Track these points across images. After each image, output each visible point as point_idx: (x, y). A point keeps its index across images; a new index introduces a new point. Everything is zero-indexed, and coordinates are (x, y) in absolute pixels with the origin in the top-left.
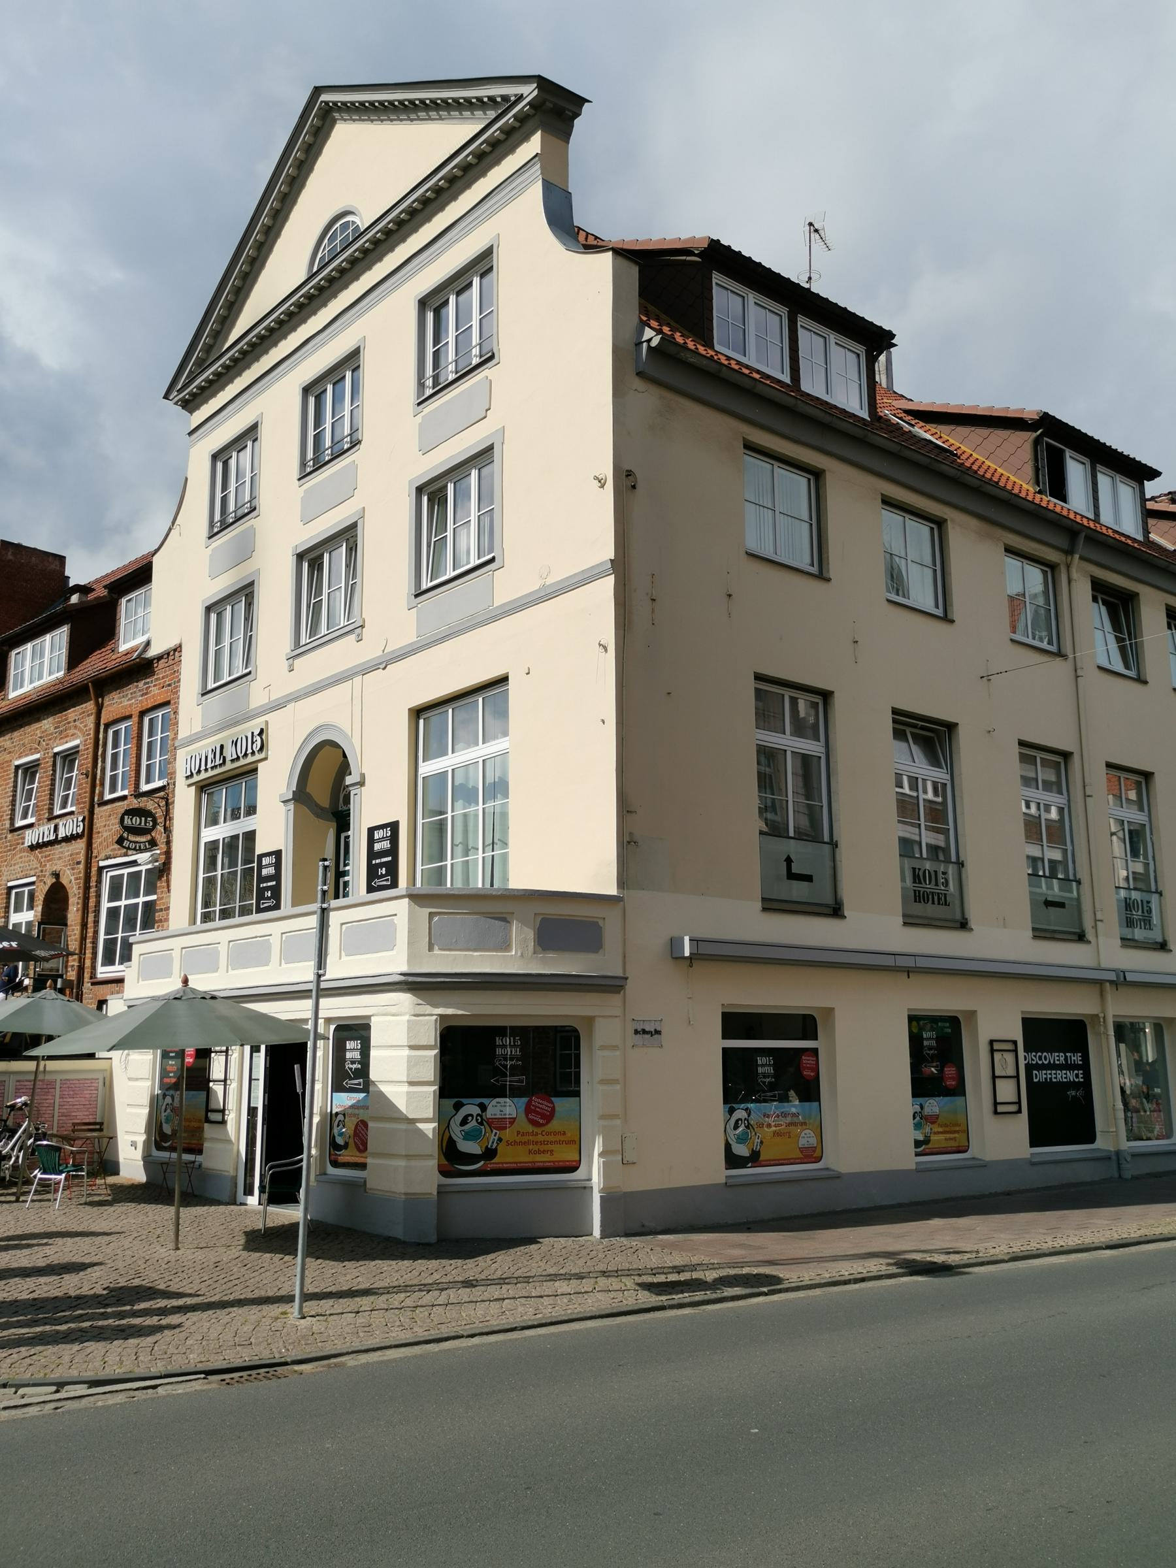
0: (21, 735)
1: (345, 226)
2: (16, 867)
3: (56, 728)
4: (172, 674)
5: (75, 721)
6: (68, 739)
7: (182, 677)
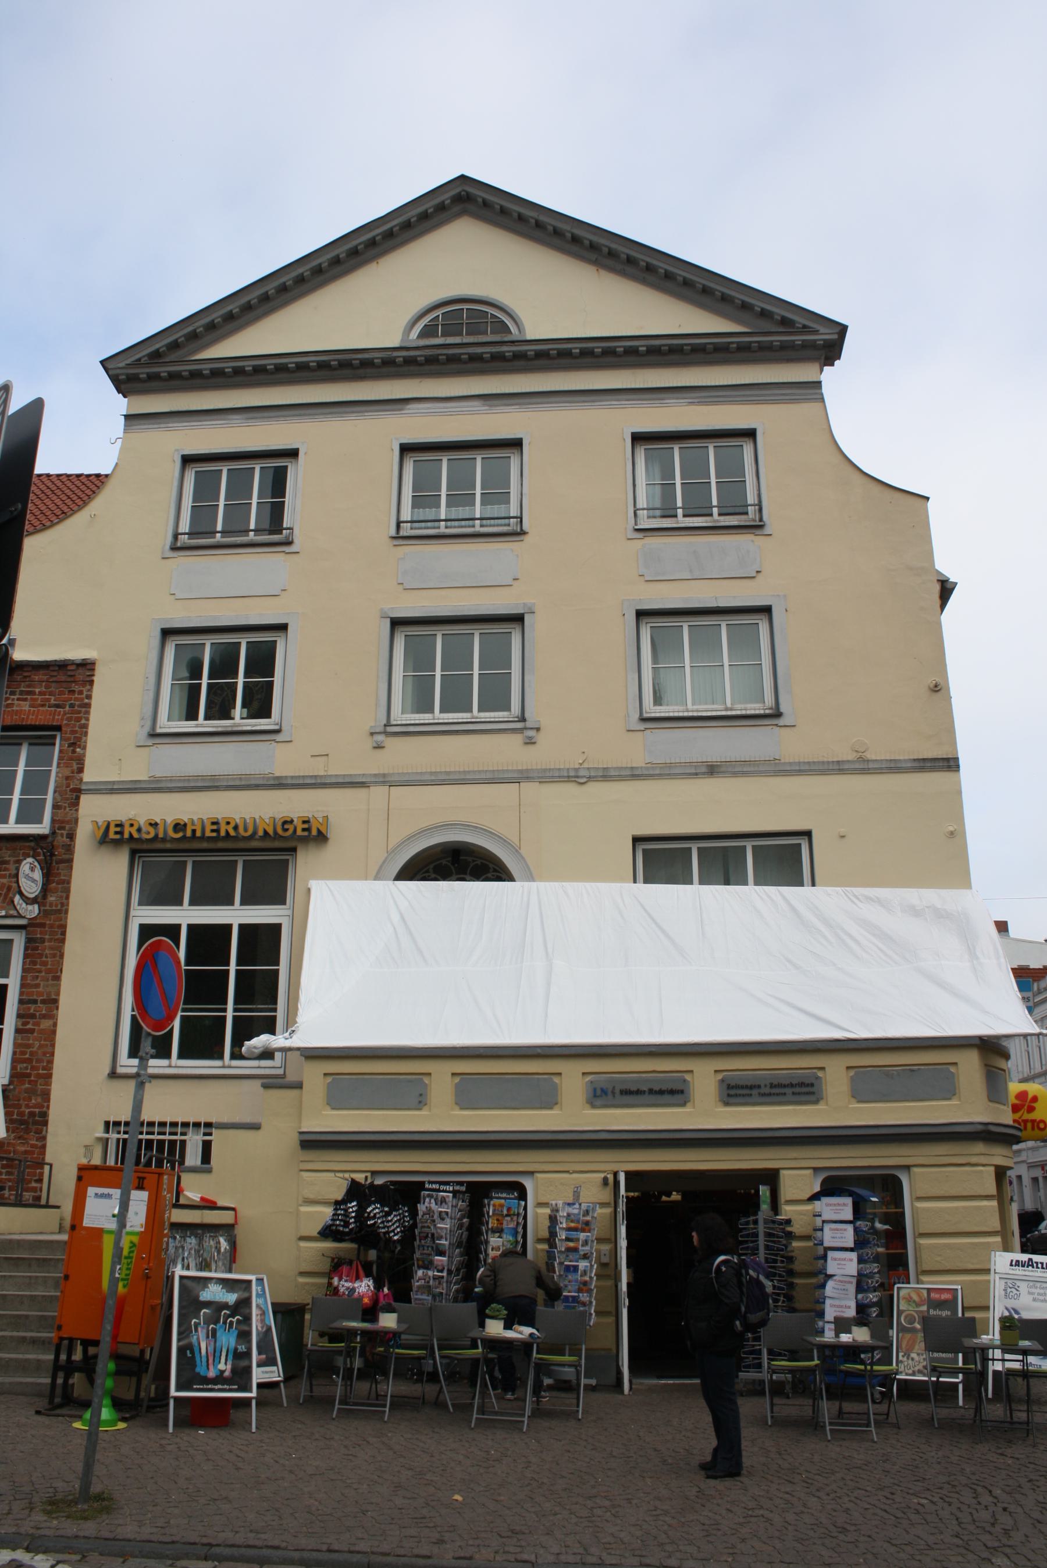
7: (95, 702)
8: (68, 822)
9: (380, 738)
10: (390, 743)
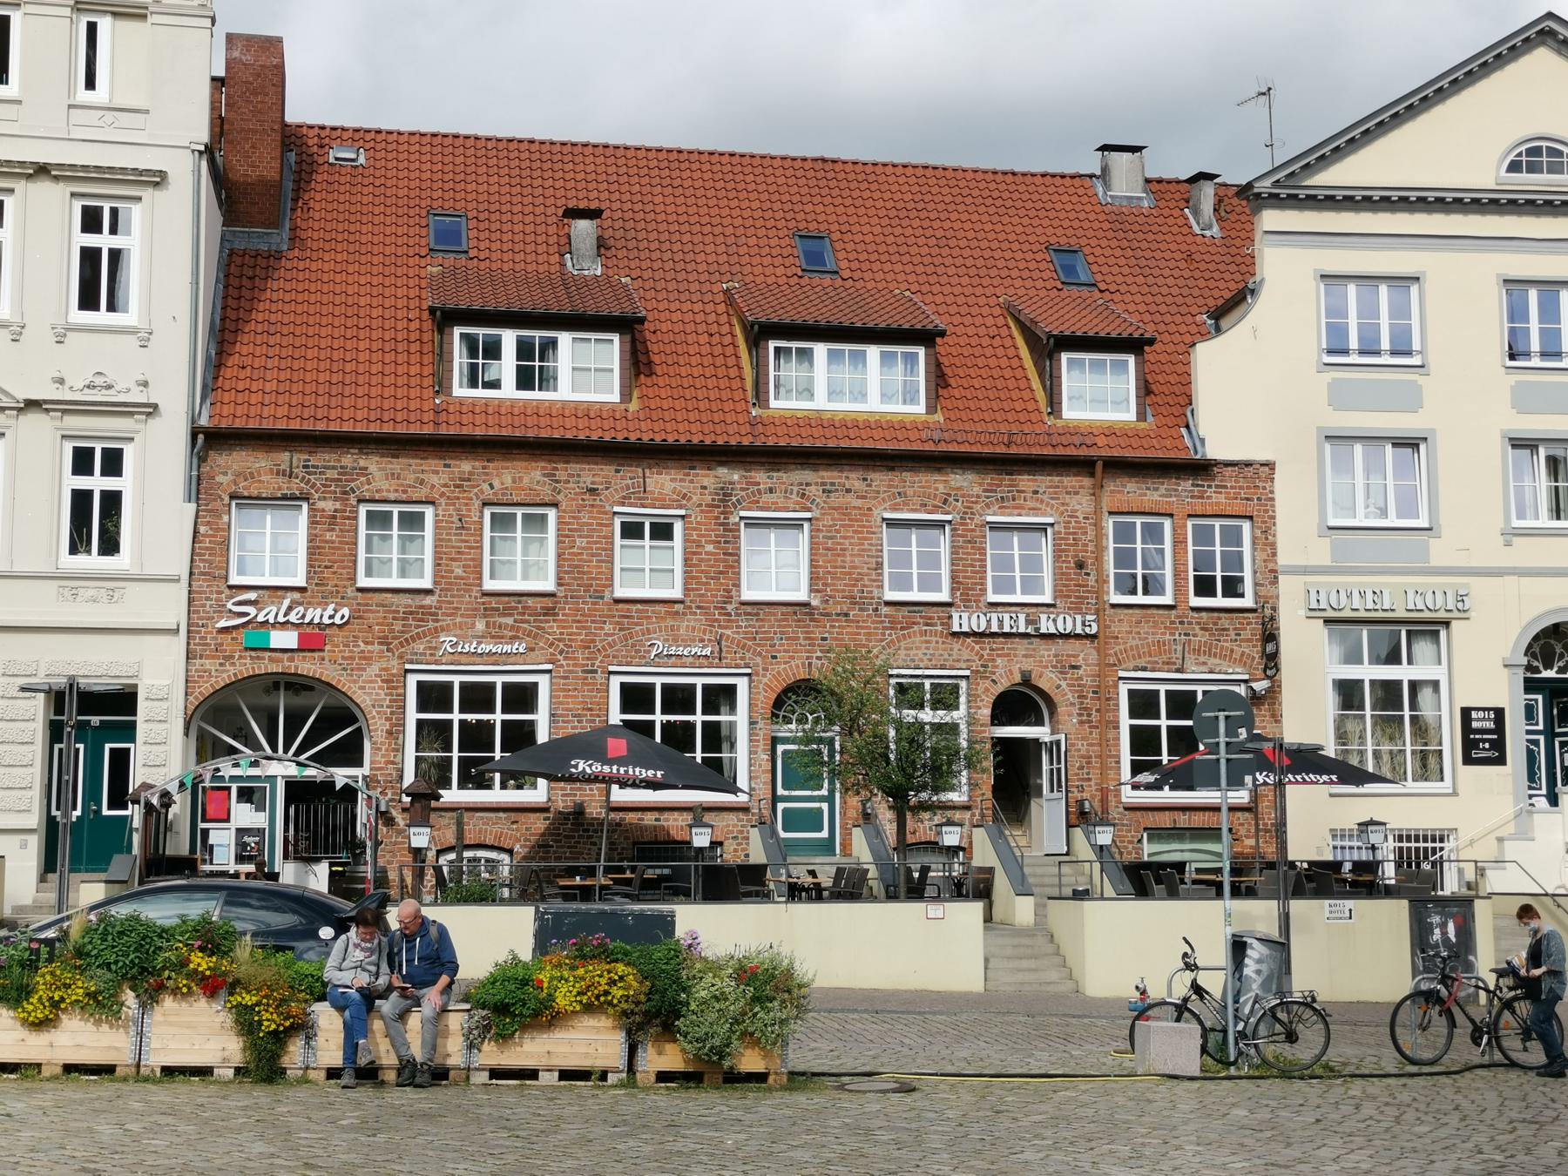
0: (890, 480)
2: (912, 653)
4: (1248, 488)
5: (1036, 492)
6: (1023, 512)
7: (1278, 495)
8: (1271, 597)
9: (1508, 537)
10: (1516, 540)
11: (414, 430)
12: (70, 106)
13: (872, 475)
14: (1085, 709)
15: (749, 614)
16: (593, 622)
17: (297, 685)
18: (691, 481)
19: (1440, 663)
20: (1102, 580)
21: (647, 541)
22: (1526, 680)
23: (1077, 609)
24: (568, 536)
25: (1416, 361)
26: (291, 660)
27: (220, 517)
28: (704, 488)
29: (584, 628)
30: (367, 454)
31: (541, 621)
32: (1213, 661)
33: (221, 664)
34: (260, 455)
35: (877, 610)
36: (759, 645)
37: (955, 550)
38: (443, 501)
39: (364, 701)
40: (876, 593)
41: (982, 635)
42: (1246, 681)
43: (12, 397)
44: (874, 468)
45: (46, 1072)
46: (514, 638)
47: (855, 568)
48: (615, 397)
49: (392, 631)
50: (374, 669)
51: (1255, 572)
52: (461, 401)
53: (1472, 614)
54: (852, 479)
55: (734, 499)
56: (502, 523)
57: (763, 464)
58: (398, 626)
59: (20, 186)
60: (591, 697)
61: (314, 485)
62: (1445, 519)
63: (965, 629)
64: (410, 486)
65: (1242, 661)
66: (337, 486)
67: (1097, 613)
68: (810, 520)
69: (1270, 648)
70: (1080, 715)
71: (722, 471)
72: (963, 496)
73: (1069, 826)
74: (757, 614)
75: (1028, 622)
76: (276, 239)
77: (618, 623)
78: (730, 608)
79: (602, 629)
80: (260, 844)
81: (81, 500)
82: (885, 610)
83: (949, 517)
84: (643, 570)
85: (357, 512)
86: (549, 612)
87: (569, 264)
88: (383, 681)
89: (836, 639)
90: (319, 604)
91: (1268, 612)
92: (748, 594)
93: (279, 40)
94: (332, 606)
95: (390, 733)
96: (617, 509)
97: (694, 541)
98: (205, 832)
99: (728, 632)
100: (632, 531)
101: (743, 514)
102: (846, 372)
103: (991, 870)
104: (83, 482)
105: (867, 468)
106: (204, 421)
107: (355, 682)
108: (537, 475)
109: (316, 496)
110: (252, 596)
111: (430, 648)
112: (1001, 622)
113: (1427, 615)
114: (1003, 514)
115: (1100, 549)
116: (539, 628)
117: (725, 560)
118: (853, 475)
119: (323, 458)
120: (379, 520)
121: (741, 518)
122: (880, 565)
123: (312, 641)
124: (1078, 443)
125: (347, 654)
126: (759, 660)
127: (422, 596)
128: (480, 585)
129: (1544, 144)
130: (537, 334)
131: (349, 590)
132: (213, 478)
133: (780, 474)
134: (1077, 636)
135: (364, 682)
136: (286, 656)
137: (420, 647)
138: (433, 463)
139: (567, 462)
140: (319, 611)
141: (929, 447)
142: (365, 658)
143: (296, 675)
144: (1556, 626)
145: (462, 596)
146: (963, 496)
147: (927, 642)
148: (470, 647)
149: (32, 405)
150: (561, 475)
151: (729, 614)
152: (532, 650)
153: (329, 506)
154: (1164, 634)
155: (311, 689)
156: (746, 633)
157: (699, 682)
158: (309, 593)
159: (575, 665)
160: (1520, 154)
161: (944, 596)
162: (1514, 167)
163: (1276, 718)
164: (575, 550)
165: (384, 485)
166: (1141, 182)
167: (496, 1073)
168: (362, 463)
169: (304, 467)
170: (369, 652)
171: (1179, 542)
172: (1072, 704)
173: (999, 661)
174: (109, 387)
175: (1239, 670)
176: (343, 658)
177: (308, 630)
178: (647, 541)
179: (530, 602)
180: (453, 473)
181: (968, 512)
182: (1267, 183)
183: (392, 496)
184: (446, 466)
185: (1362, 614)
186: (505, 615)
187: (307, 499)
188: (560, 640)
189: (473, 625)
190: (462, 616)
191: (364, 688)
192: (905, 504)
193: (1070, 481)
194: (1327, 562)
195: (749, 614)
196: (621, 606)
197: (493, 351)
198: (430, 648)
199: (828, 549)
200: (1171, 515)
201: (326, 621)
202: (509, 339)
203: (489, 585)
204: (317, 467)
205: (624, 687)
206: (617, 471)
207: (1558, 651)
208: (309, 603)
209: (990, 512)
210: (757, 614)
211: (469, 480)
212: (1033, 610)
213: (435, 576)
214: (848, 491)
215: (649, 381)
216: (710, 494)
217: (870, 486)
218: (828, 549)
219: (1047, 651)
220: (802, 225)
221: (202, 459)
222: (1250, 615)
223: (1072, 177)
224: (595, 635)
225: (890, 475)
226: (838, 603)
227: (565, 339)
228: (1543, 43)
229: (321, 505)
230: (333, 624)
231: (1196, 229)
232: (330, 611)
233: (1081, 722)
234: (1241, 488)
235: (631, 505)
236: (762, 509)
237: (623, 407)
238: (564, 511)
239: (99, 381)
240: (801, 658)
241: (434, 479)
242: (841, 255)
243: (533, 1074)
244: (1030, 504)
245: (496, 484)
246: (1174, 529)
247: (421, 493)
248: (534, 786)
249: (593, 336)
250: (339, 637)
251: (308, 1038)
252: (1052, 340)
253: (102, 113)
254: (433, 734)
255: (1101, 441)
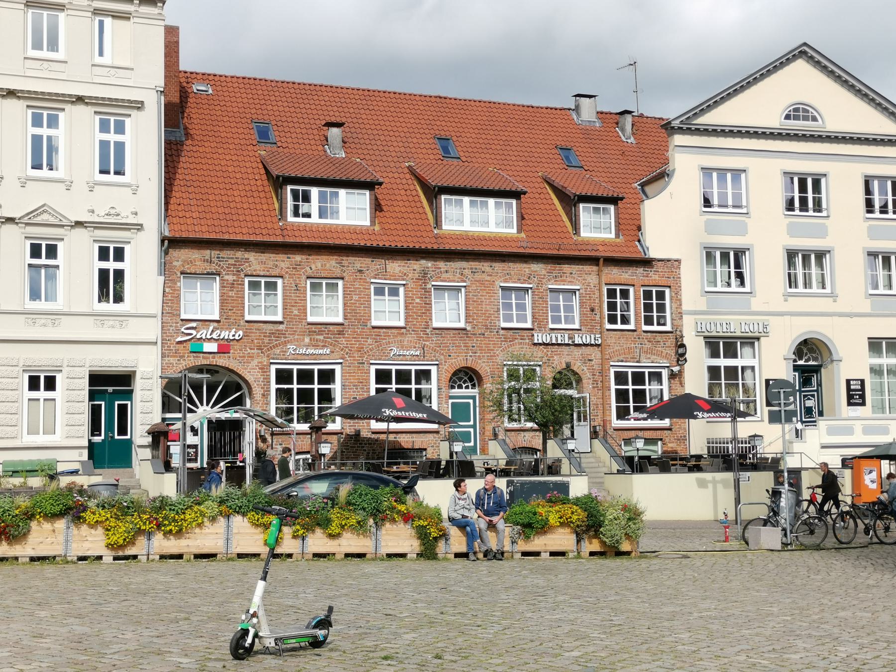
1: (808, 111)
3: (548, 272)
5: (571, 273)
7: (682, 276)
10: (790, 298)
11: (272, 239)
12: (93, 65)
13: (494, 264)
14: (595, 381)
15: (436, 334)
16: (362, 338)
17: (211, 370)
18: (408, 267)
19: (754, 357)
20: (602, 317)
21: (387, 297)
22: (794, 366)
23: (591, 331)
24: (349, 294)
25: (744, 211)
26: (214, 358)
27: (176, 284)
28: (415, 270)
29: (358, 341)
30: (248, 251)
31: (337, 338)
32: (653, 357)
33: (178, 360)
34: (196, 251)
35: (497, 332)
36: (442, 350)
37: (534, 302)
38: (287, 276)
39: (250, 379)
40: (497, 324)
41: (547, 344)
42: (668, 367)
43: (68, 219)
44: (496, 261)
45: (338, 557)
46: (324, 346)
47: (487, 311)
48: (368, 223)
49: (263, 343)
50: (255, 362)
51: (672, 314)
52: (293, 224)
53: (770, 334)
54: (485, 266)
55: (429, 276)
56: (315, 287)
57: (442, 258)
58: (266, 340)
59: (68, 107)
60: (362, 376)
61: (223, 267)
62: (758, 289)
63: (540, 341)
64: (270, 268)
65: (666, 357)
66: (234, 268)
67: (601, 333)
68: (465, 287)
69: (681, 351)
70: (593, 384)
71: (423, 262)
72: (537, 275)
73: (591, 438)
74: (441, 334)
75: (569, 338)
76: (178, 134)
77: (374, 339)
78: (428, 331)
79: (367, 341)
80: (196, 453)
81: (103, 275)
82: (502, 332)
83: (531, 286)
84: (385, 312)
85: (244, 281)
86: (341, 333)
87: (328, 151)
88: (259, 368)
89: (479, 347)
90: (227, 329)
91: (678, 333)
92: (436, 324)
93: (178, 28)
94: (234, 330)
95: (263, 395)
96: (373, 280)
97: (410, 297)
98: (168, 447)
99: (427, 343)
100: (379, 292)
101: (433, 283)
102: (479, 212)
103: (559, 460)
104: (104, 265)
105: (492, 261)
106: (167, 234)
107: (246, 369)
108: (333, 263)
109: (224, 273)
110: (194, 325)
111: (283, 351)
112: (557, 338)
113: (750, 334)
114: (556, 284)
115: (601, 301)
116: (336, 341)
117: (425, 307)
118: (486, 264)
119: (226, 253)
120: (254, 286)
121: (433, 285)
122: (499, 309)
123: (224, 349)
124: (590, 249)
125: (241, 355)
126: (442, 357)
127: (278, 325)
128: (306, 319)
129: (801, 106)
130: (329, 190)
131: (242, 322)
132: (172, 263)
133: (451, 263)
134: (592, 345)
135: (250, 369)
136: (211, 356)
137: (277, 351)
138: (281, 257)
139: (348, 256)
140: (227, 333)
141: (521, 251)
142: (250, 357)
143: (216, 365)
144: (805, 341)
145: (298, 325)
146: (537, 275)
147: (522, 348)
148: (302, 351)
149: (79, 224)
150: (345, 263)
151: (428, 334)
152: (333, 352)
153: (230, 278)
154: (631, 344)
155: (217, 372)
156: (436, 343)
157: (413, 368)
158: (221, 323)
159: (354, 360)
160: (790, 111)
161: (529, 325)
162: (788, 117)
163: (682, 384)
164: (353, 301)
165: (258, 267)
166: (595, 113)
167: (525, 554)
168: (246, 256)
169: (218, 258)
170: (252, 353)
171: (636, 299)
172: (590, 379)
173: (555, 357)
174: (118, 215)
175: (665, 361)
176: (240, 357)
177: (222, 342)
178: (387, 297)
179: (331, 328)
180: (292, 261)
181: (540, 283)
182: (678, 122)
183: (262, 273)
184: (288, 258)
185: (721, 334)
186: (319, 335)
187: (219, 275)
188: (346, 347)
189: (304, 340)
190: (298, 335)
191: (250, 372)
192: (510, 279)
193: (587, 268)
194: (705, 308)
195: (436, 334)
196: (375, 330)
197: (307, 198)
198: (283, 351)
199: (474, 301)
200: (634, 285)
201: (231, 338)
202: (315, 192)
203: (310, 319)
204: (224, 258)
205: (377, 371)
206: (372, 261)
207: (805, 352)
208: (222, 328)
209: (550, 283)
210: (441, 334)
211: (300, 265)
212: (571, 332)
213: (284, 314)
214: (483, 272)
215: (381, 214)
216: (418, 273)
217: (493, 269)
218: (474, 301)
219: (577, 352)
220: (437, 132)
221: (166, 253)
222: (670, 334)
223: (561, 110)
224: (363, 344)
225: (503, 264)
226: (480, 328)
227: (342, 192)
228: (801, 57)
229: (226, 277)
230: (234, 339)
231: (623, 139)
232: (233, 333)
233: (594, 387)
234: (665, 272)
235: (379, 279)
236: (442, 281)
237: (372, 228)
238: (347, 282)
239: (113, 212)
240: (462, 356)
241: (283, 265)
242: (459, 149)
243: (537, 554)
244: (568, 279)
245: (313, 267)
246: (635, 292)
247: (276, 272)
248: (334, 421)
249: (357, 191)
250: (237, 346)
251: (447, 540)
252: (576, 198)
253: (109, 69)
254: (284, 395)
255: (601, 248)
